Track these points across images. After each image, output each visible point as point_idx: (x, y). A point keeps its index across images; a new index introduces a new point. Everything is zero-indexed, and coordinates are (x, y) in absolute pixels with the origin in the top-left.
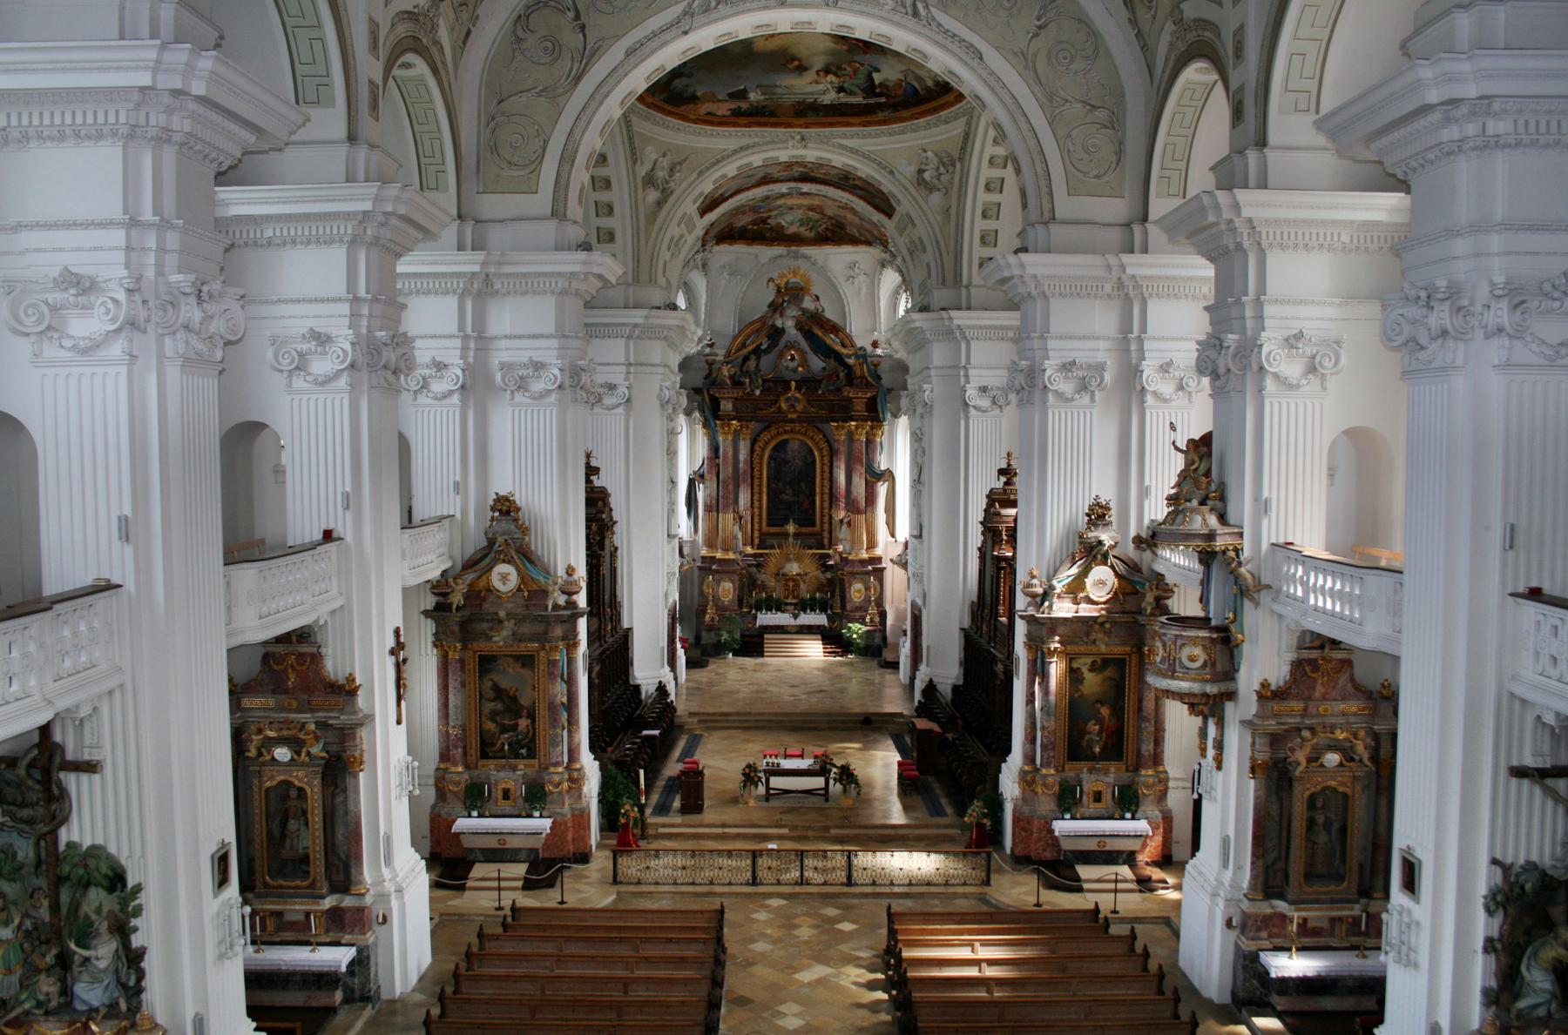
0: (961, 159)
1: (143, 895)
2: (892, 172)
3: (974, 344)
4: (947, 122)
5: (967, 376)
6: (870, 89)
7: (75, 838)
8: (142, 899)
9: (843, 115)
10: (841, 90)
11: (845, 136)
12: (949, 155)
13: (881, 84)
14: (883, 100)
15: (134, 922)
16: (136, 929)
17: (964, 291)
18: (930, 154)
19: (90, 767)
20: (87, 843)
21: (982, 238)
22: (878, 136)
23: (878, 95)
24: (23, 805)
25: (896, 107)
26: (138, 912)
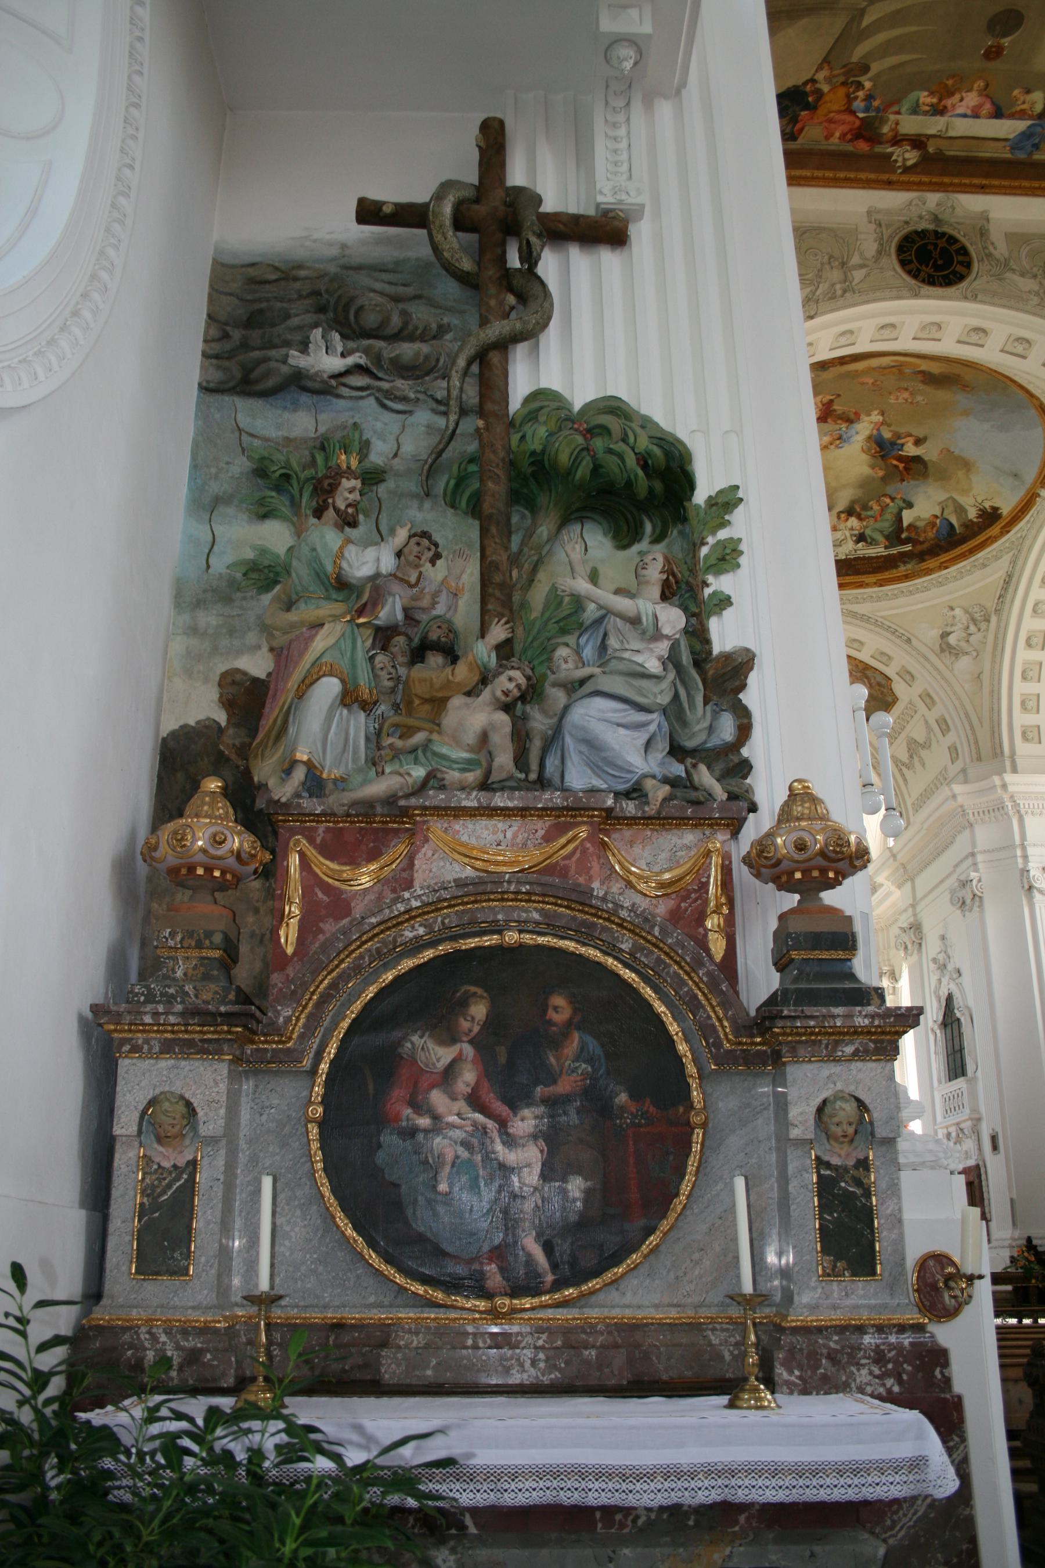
0: (998, 611)
1: (738, 516)
2: (909, 641)
3: (1028, 820)
4: (984, 566)
5: (1025, 857)
6: (896, 534)
7: (552, 379)
8: (740, 525)
9: (858, 572)
10: (861, 538)
11: (857, 600)
12: (983, 608)
13: (910, 526)
14: (908, 548)
15: (718, 584)
16: (724, 602)
17: (1008, 764)
18: (958, 612)
19: (605, 231)
20: (581, 395)
21: (1023, 703)
22: (896, 596)
23: (904, 542)
24: (396, 337)
25: (921, 557)
26: (728, 557)
